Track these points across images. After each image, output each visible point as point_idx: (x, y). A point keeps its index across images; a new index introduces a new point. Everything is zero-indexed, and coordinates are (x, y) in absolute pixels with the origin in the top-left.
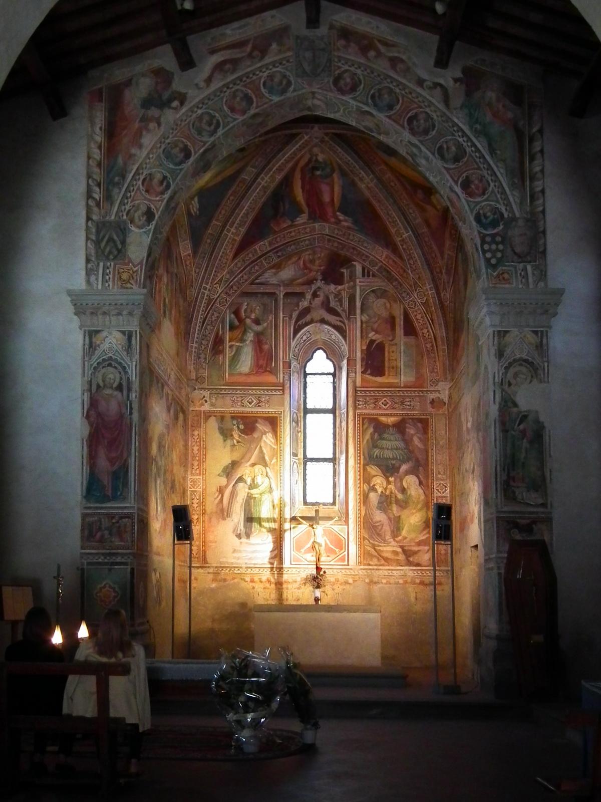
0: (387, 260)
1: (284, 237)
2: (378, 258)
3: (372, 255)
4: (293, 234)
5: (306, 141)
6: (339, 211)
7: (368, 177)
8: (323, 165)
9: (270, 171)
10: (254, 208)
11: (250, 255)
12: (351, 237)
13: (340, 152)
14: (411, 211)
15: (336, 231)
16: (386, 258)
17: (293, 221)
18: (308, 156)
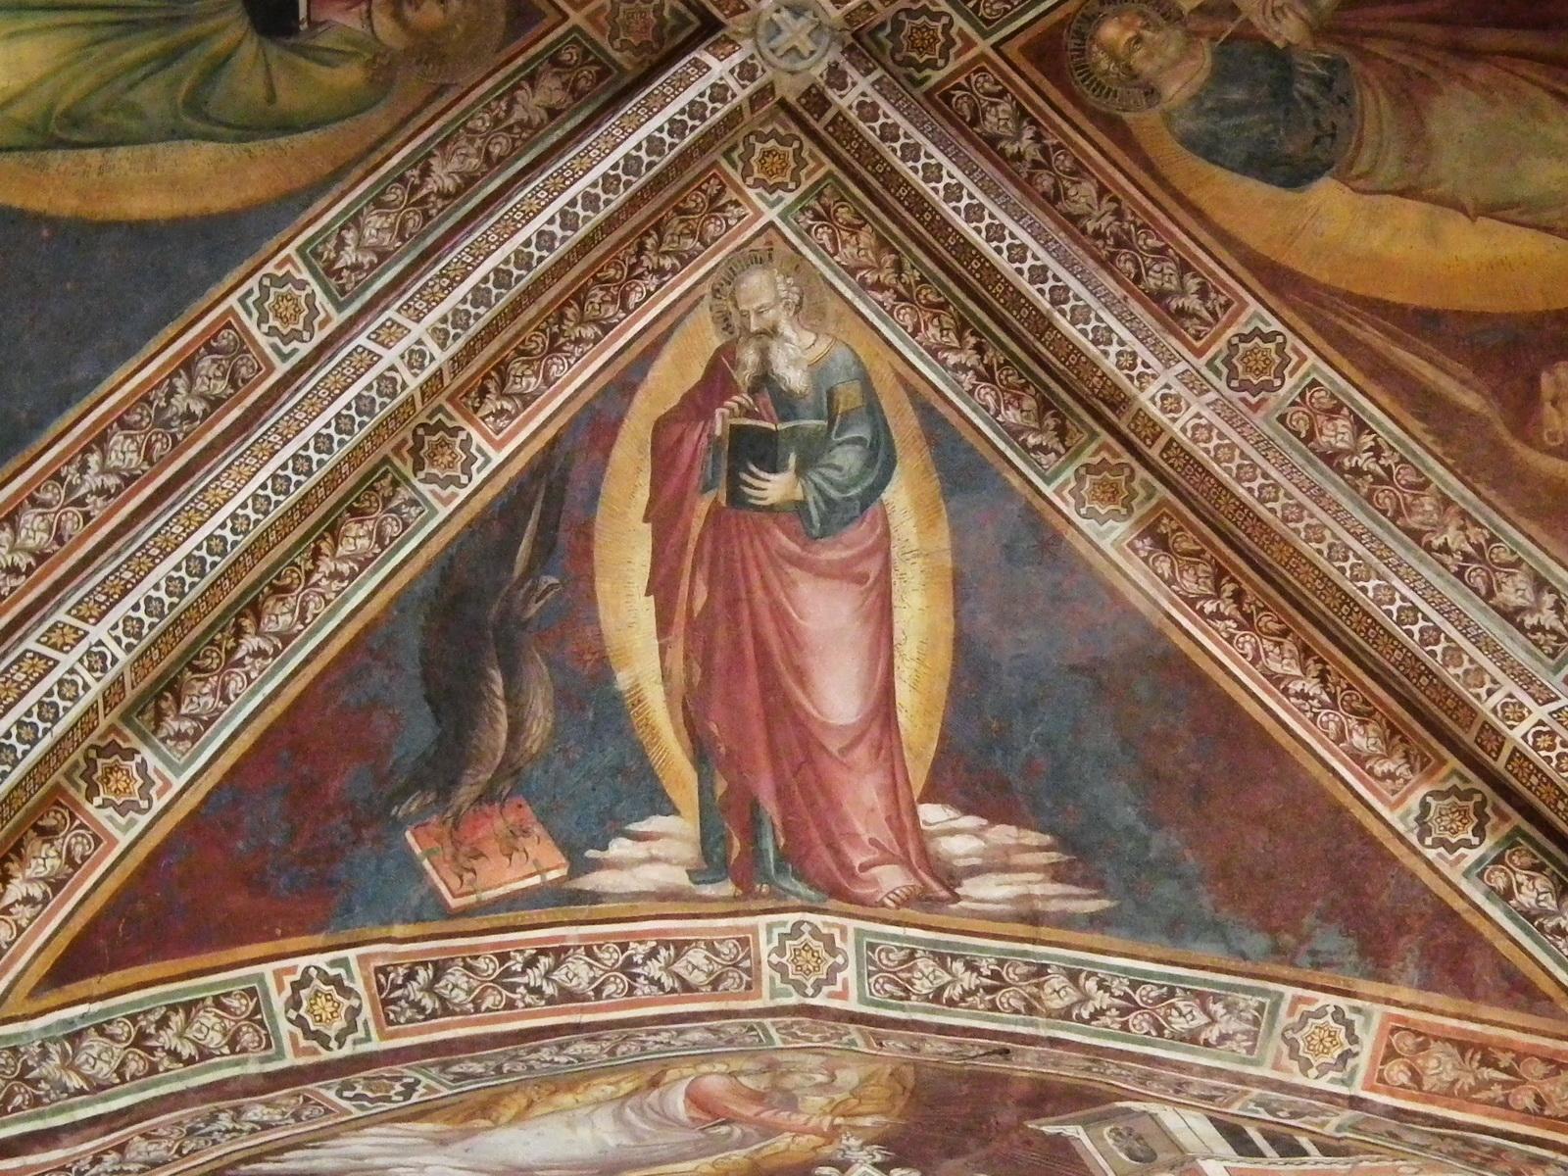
0: (1398, 1073)
1: (504, 980)
2: (1323, 1084)
3: (1264, 1082)
4: (578, 973)
5: (719, 92)
6: (931, 795)
7: (1167, 367)
8: (812, 423)
9: (454, 284)
10: (286, 638)
11: (210, 1028)
12: (1057, 992)
13: (953, 193)
14: (1514, 591)
15: (926, 976)
16: (1391, 1054)
17: (580, 866)
18: (702, 339)
